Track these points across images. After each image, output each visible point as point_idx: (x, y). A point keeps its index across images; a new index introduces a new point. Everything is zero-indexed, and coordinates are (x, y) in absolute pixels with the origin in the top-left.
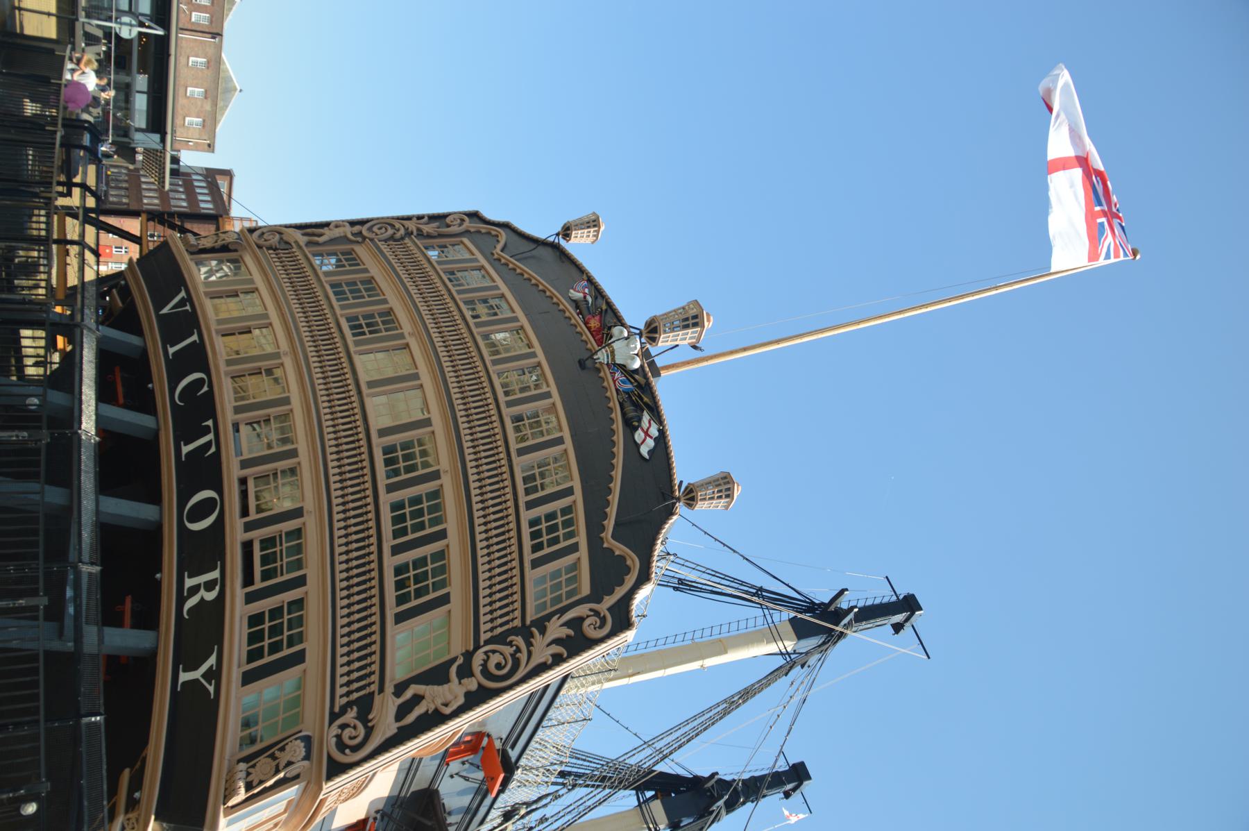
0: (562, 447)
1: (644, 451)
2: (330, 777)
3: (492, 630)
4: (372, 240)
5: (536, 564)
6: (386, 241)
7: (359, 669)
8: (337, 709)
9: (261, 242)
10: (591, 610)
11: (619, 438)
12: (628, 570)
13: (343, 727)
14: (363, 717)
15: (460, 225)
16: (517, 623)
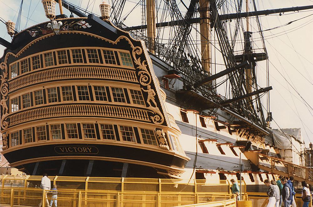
0: (85, 50)
1: (89, 26)
2: (167, 125)
3: (135, 79)
5: (119, 64)
6: (9, 90)
7: (141, 114)
8: (150, 121)
9: (6, 127)
10: (134, 52)
11: (84, 33)
12: (124, 39)
13: (155, 120)
14: (153, 115)
15: (4, 65)
16: (135, 72)
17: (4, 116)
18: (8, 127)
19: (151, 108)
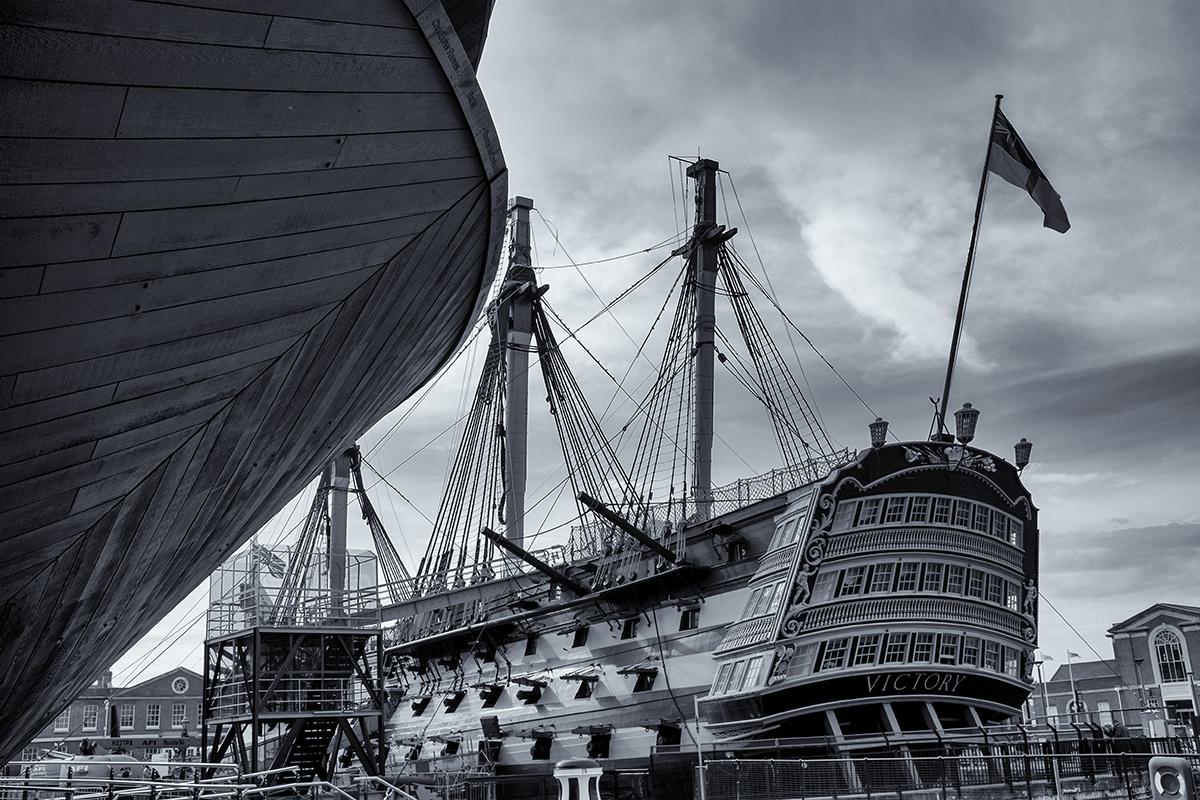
4: (823, 561)
17: (798, 608)
18: (800, 634)
19: (1026, 615)
